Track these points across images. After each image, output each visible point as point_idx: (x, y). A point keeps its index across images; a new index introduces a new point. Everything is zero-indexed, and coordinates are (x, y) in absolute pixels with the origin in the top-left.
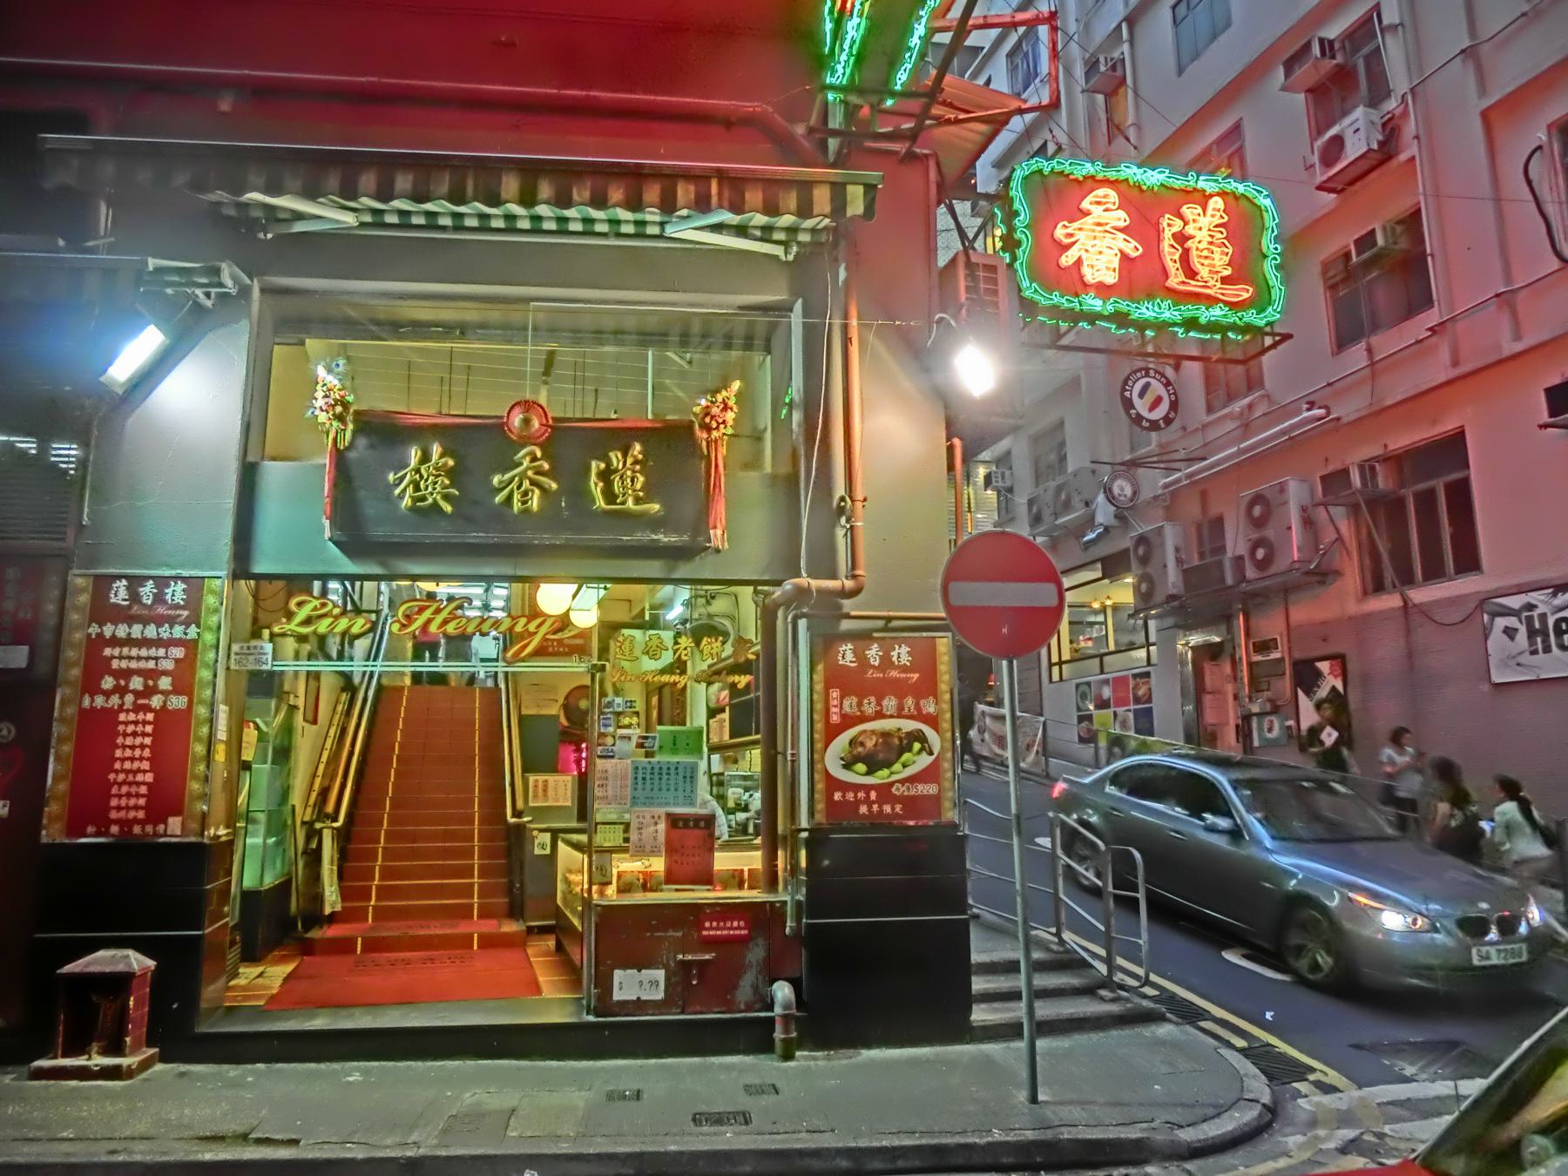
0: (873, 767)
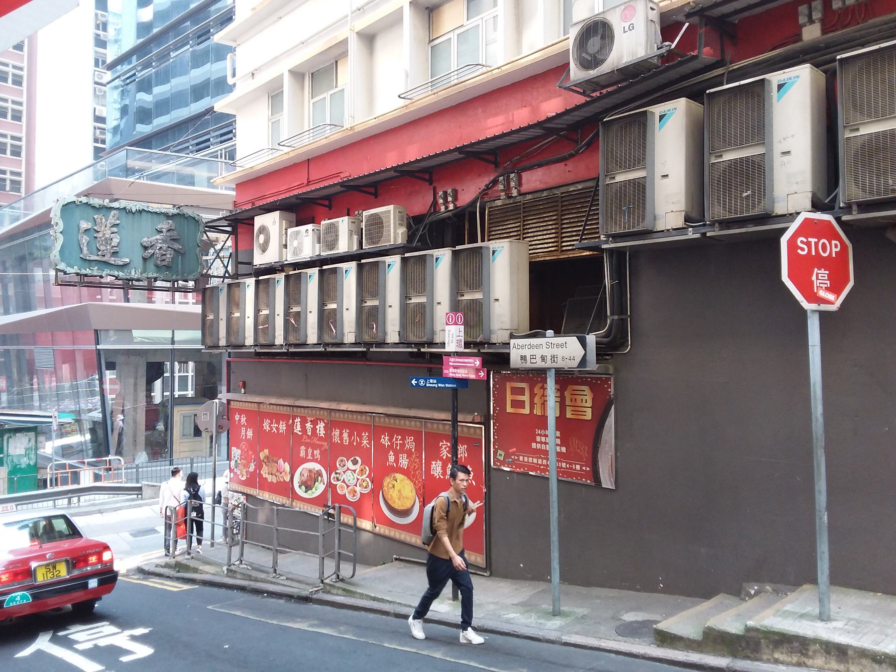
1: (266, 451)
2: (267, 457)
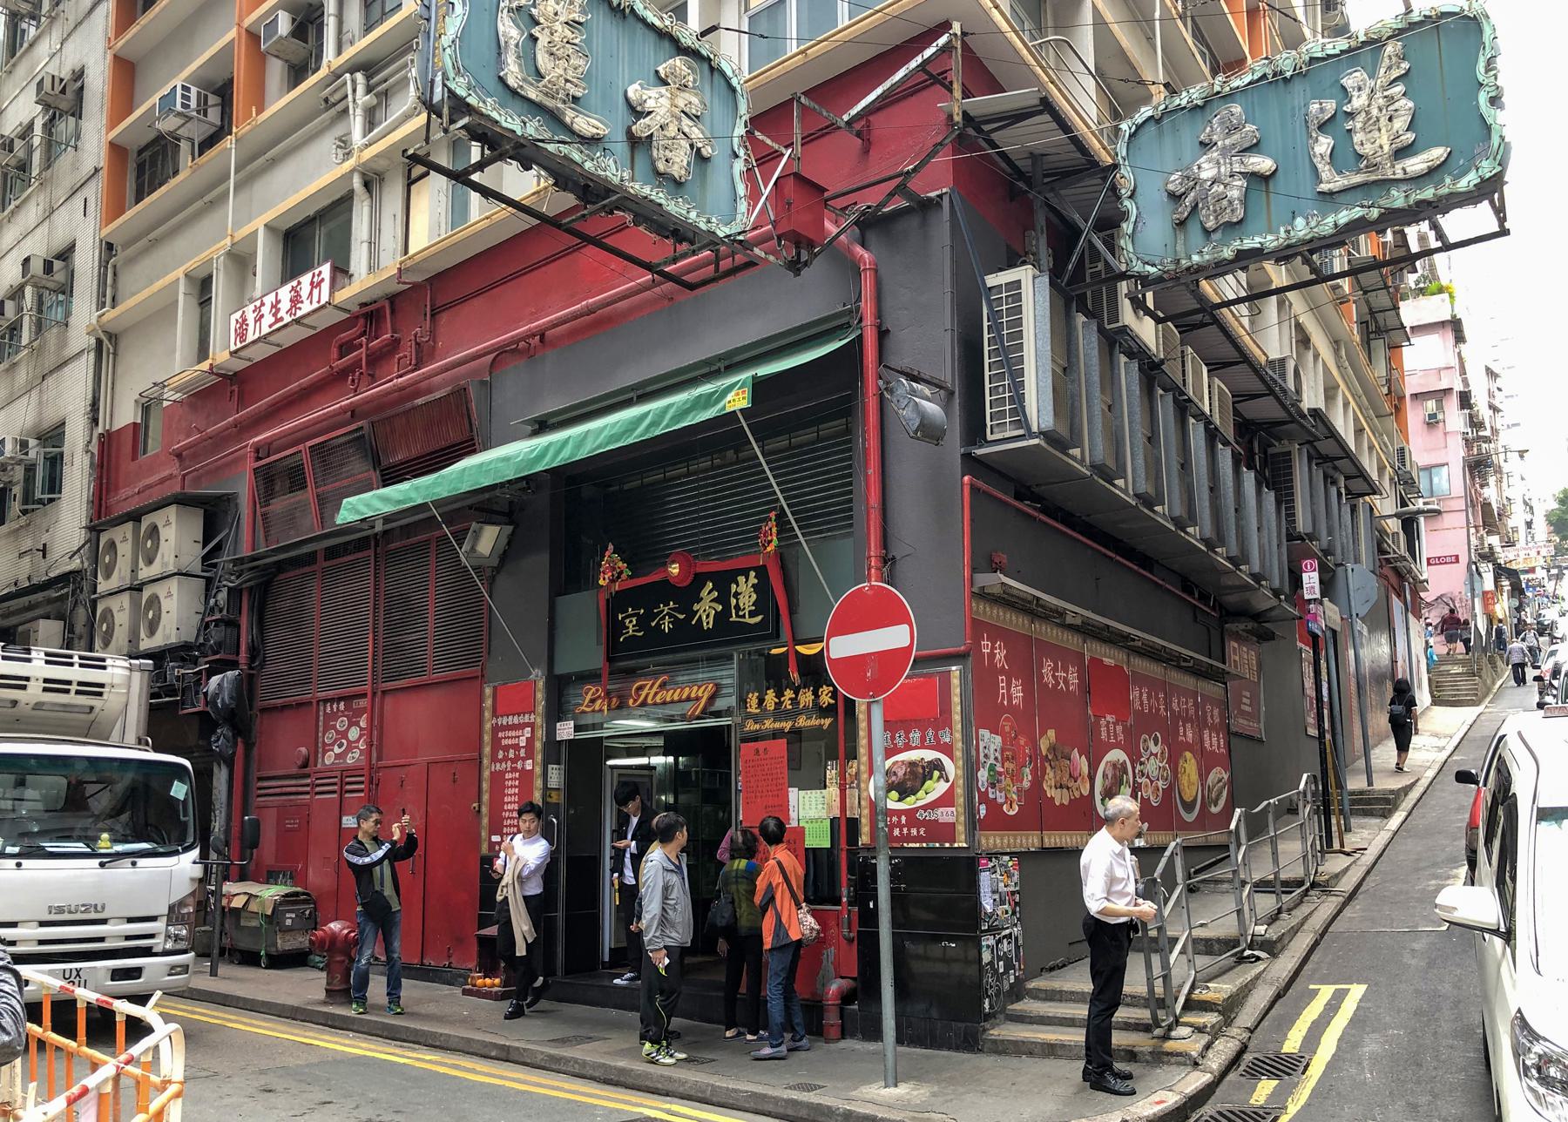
0: (904, 791)
1: (1051, 733)
2: (1053, 749)
